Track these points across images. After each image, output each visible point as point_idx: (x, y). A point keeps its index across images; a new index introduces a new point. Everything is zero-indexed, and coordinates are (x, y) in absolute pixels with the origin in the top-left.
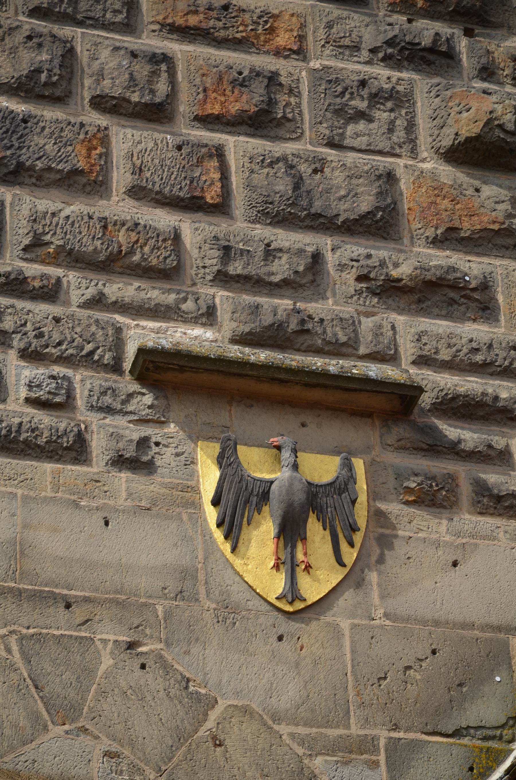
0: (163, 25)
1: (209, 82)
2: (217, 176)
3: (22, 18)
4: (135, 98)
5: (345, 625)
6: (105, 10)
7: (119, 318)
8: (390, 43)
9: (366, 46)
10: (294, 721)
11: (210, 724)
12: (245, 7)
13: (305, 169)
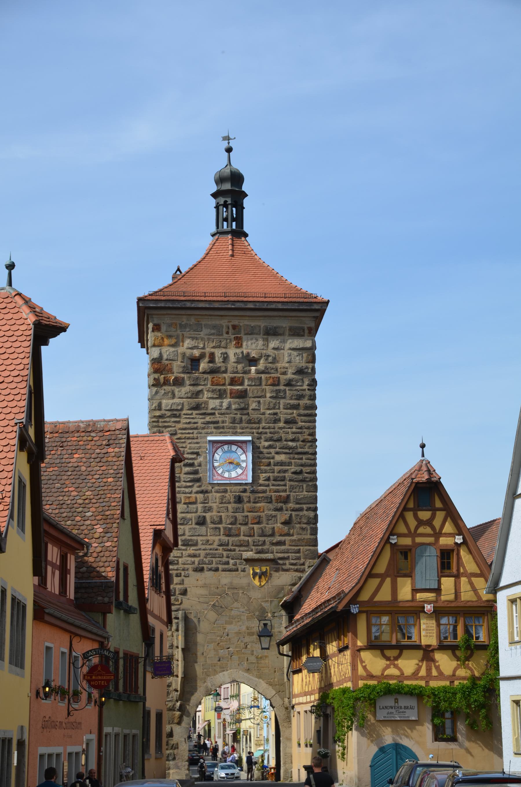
5: (266, 587)
7: (242, 552)
10: (260, 599)
13: (263, 528)
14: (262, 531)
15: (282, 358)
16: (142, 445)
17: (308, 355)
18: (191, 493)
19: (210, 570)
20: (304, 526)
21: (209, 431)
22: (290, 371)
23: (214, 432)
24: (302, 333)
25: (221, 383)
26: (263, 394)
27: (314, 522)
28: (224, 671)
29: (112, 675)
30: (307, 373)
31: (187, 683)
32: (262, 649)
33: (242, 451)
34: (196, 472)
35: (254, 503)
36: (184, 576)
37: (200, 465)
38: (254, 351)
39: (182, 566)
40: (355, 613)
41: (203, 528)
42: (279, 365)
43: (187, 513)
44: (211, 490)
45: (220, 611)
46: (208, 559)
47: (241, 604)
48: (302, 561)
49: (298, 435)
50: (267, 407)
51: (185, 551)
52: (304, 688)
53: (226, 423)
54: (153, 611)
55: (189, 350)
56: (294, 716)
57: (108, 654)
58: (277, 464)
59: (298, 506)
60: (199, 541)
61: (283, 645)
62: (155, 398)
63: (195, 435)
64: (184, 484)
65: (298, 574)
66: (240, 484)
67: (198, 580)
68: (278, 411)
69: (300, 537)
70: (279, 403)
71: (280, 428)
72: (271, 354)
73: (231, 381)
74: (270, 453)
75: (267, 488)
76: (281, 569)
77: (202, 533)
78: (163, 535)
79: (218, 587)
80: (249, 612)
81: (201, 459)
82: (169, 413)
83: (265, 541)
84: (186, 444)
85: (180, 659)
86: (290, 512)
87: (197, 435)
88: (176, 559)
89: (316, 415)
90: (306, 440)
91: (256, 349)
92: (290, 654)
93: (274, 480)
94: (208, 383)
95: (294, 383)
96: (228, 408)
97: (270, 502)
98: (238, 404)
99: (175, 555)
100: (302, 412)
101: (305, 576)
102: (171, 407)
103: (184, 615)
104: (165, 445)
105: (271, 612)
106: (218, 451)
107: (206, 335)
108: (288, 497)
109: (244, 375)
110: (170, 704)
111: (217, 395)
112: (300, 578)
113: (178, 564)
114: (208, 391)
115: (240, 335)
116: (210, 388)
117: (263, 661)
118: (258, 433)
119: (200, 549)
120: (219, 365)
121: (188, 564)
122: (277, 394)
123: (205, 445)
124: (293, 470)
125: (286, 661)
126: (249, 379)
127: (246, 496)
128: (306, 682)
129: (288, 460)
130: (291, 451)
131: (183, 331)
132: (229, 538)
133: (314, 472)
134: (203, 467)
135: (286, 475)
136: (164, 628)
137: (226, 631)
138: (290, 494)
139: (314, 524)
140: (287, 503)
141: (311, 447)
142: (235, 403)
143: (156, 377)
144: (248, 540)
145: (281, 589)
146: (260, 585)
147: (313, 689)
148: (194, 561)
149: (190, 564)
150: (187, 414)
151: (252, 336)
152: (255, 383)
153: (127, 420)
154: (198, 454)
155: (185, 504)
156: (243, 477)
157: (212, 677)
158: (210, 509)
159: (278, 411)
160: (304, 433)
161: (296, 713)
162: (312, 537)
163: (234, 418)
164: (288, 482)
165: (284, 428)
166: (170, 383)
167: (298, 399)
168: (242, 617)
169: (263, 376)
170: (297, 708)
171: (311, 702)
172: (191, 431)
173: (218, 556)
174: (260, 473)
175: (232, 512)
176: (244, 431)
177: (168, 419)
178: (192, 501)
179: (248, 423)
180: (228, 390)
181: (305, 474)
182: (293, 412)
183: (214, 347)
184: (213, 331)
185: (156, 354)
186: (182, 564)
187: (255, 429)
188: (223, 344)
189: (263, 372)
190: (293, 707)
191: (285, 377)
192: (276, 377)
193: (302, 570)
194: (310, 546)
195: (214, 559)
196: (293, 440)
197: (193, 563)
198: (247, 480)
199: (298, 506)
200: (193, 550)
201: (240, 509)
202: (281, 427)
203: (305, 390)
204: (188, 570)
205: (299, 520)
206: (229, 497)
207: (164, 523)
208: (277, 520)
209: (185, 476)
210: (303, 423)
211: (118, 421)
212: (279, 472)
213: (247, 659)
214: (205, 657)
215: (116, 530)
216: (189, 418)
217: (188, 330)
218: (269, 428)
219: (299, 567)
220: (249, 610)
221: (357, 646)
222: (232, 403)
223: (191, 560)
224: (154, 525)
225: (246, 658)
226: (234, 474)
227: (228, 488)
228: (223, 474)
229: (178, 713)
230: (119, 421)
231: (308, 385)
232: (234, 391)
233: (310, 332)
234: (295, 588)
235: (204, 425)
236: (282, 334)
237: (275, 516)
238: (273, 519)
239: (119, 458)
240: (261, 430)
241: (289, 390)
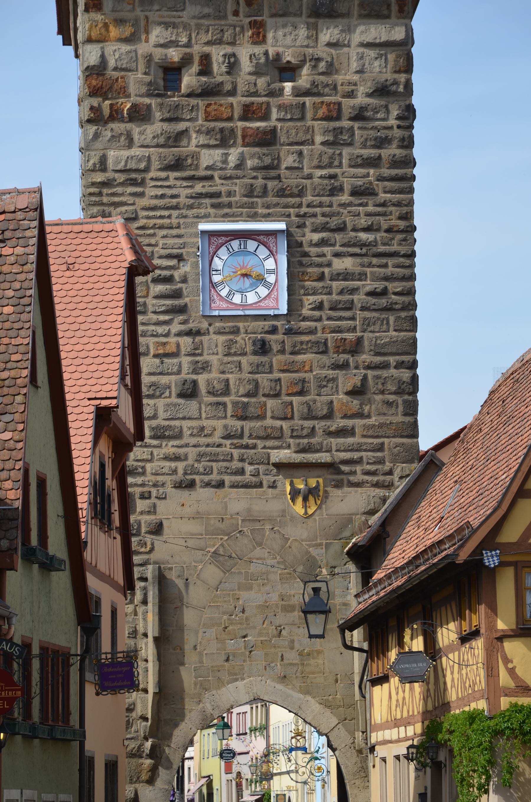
1: (289, 384)
2: (290, 410)
4: (272, 393)
5: (317, 518)
7: (269, 451)
8: (332, 364)
9: (327, 366)
10: (306, 541)
11: (289, 544)
13: (311, 403)
14: (309, 408)
15: (345, 65)
16: (69, 241)
17: (398, 56)
18: (167, 335)
19: (208, 484)
20: (392, 398)
21: (202, 211)
22: (362, 90)
23: (212, 215)
24: (386, 12)
25: (225, 116)
26: (309, 137)
27: (411, 390)
28: (236, 680)
29: (18, 690)
30: (395, 94)
31: (165, 704)
32: (311, 636)
33: (268, 253)
34: (177, 294)
35: (292, 353)
36: (156, 497)
37: (184, 280)
38: (290, 50)
39: (153, 478)
40: (492, 566)
41: (193, 404)
42: (339, 78)
43: (161, 374)
44: (208, 329)
45: (229, 564)
46: (202, 463)
47: (268, 550)
48: (388, 466)
49: (377, 218)
50: (315, 162)
51: (158, 449)
52: (393, 713)
53: (235, 196)
54: (96, 566)
55: (160, 50)
56: (374, 766)
57: (10, 649)
58: (337, 277)
59: (378, 359)
60: (185, 429)
61: (351, 630)
62: (93, 148)
63: (174, 221)
64: (155, 317)
65: (380, 492)
66: (265, 317)
67: (183, 505)
68: (338, 171)
69: (382, 419)
70: (340, 154)
71: (343, 205)
72: (324, 55)
73: (244, 111)
74: (324, 255)
75: (319, 325)
76: (345, 482)
77: (190, 414)
78: (113, 417)
79: (222, 519)
80: (285, 565)
81: (186, 268)
82: (121, 178)
83: (313, 428)
84: (157, 238)
85: (150, 658)
86: (362, 371)
87: (177, 221)
88: (140, 464)
89: (413, 178)
90: (395, 229)
91: (294, 46)
92: (365, 646)
93: (331, 309)
94: (197, 115)
95: (369, 114)
96: (238, 167)
97: (324, 352)
98: (259, 158)
99: (139, 458)
100: (386, 172)
101: (394, 495)
102: (126, 165)
103: (157, 573)
104: (116, 240)
105: (327, 566)
107: (194, 17)
108: (359, 341)
109: (271, 100)
110: (133, 745)
111: (216, 139)
112: (384, 500)
113: (144, 473)
114: (199, 132)
115: (259, 18)
116: (202, 126)
117: (312, 662)
118: (298, 216)
119: (187, 445)
120: (219, 79)
121: (163, 474)
122: (335, 136)
123: (195, 240)
124: (368, 289)
125: (358, 658)
126: (280, 107)
127: (276, 341)
128: (397, 701)
129: (359, 268)
130: (364, 250)
131: (147, 10)
132: (244, 423)
133: (411, 292)
134: (191, 283)
135: (355, 297)
136: (118, 597)
137: (241, 603)
138: (362, 337)
139: (410, 394)
140: (357, 353)
141: (404, 243)
142: (252, 156)
143: (96, 104)
144: (282, 427)
145: (348, 520)
146: (306, 513)
147: (411, 713)
148: (176, 468)
149: (167, 474)
150: (156, 179)
151: (285, 19)
152: (293, 115)
153: (39, 191)
154: (180, 258)
155: (155, 356)
156: (270, 303)
157: (214, 692)
158: (205, 367)
159: (338, 171)
160: (391, 213)
161: (378, 761)
162: (408, 419)
163: (252, 185)
164: (358, 312)
165: (350, 204)
166: (123, 117)
167: (379, 147)
168: (271, 577)
169: (308, 101)
170: (380, 751)
171: (406, 739)
172: (166, 213)
173: (222, 458)
174: (305, 295)
175: (250, 373)
176: (270, 211)
177: (119, 190)
178: (170, 352)
179: (278, 196)
181: (393, 296)
182: (368, 173)
183: (209, 43)
184: (206, 10)
185: (94, 58)
186: (153, 474)
187: (293, 207)
188: (227, 36)
189: (307, 93)
190: (372, 749)
191: (352, 102)
192: (334, 103)
193: (387, 484)
194: (402, 437)
195: (214, 464)
196: (368, 229)
197: (175, 471)
198: (278, 309)
199: (378, 359)
200: (173, 446)
201: (264, 366)
202: (344, 204)
203: (391, 128)
204: (163, 485)
205: (380, 386)
206: (242, 342)
207: (115, 394)
208: (337, 386)
209: (155, 301)
210: (389, 195)
211: (20, 192)
212: (341, 292)
213: (282, 655)
214: (200, 653)
215: (21, 408)
216: (161, 187)
217: (156, 7)
218: (321, 205)
219: (381, 478)
220: (284, 562)
221: (497, 631)
222: (247, 156)
223: (170, 467)
224: (95, 399)
225: (280, 655)
226: (251, 298)
227: (241, 325)
228: (231, 297)
229: (148, 762)
230: (23, 193)
231: (398, 118)
232: (250, 132)
233: (401, 10)
234: (374, 520)
235: (192, 201)
236: (347, 15)
237: (334, 380)
238: (330, 385)
239: (25, 267)
240: (304, 210)
241: (359, 128)
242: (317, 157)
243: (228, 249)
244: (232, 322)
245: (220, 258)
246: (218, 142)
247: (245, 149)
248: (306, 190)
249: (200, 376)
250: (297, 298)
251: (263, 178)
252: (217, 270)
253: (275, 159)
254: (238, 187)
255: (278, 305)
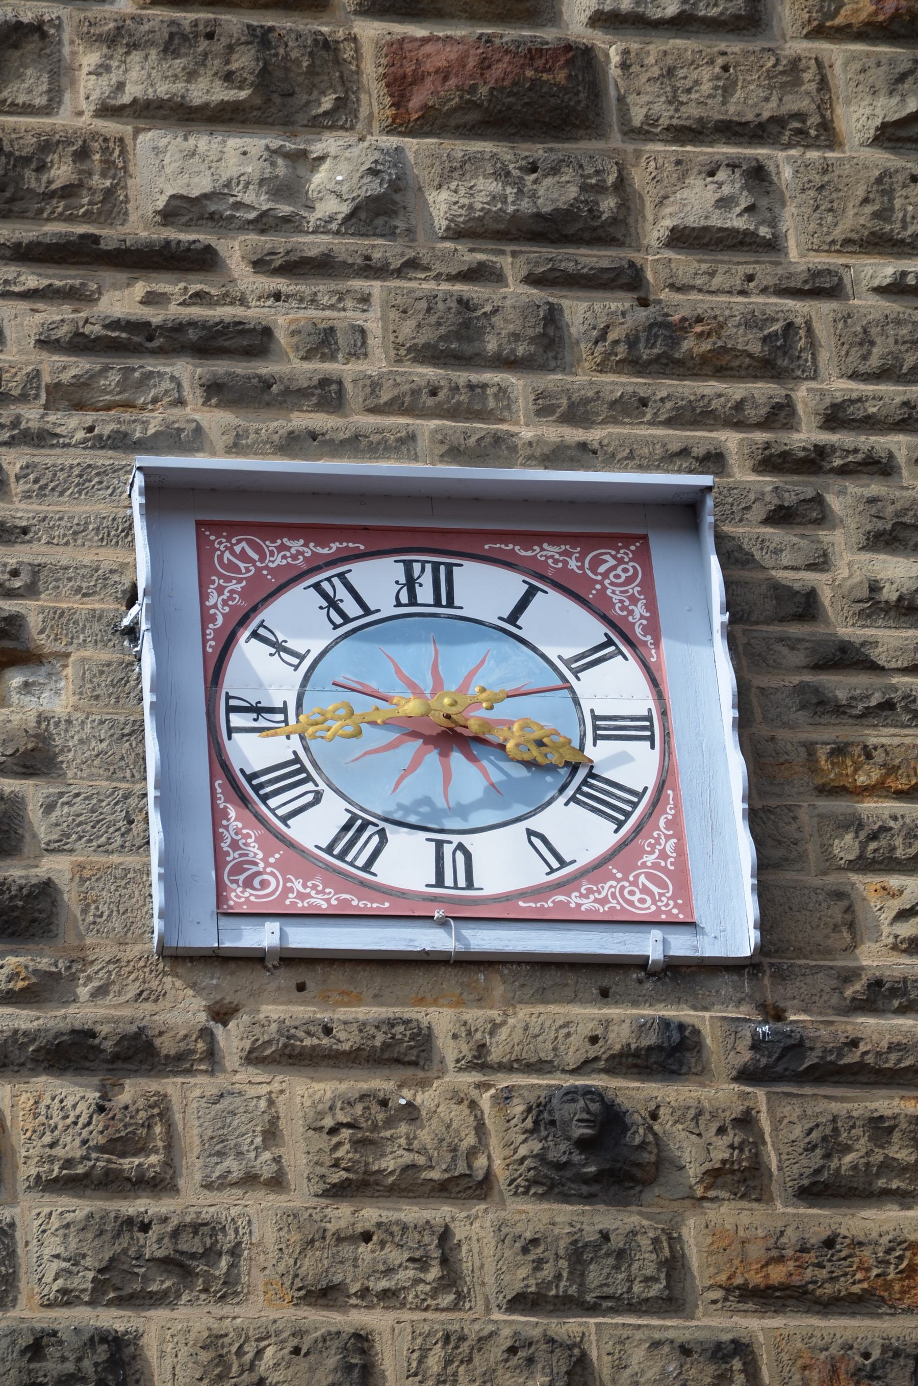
0: (728, 1290)
3: (497, 1316)
6: (630, 1280)
12: (862, 1238)
33: (597, 631)
44: (206, 1033)
53: (359, 350)
106: (271, 615)
111: (228, 77)
123: (109, 557)
174: (862, 864)
176: (595, 435)
180: (368, 52)
206: (459, 1115)
222: (422, 173)
242: (860, 192)
243: (332, 603)
244: (377, 999)
245: (279, 647)
246: (243, 94)
247: (411, 144)
248: (813, 345)
249: (159, 1315)
250: (817, 882)
251: (532, 280)
252: (258, 710)
253: (600, 189)
254: (375, 312)
255: (687, 906)
